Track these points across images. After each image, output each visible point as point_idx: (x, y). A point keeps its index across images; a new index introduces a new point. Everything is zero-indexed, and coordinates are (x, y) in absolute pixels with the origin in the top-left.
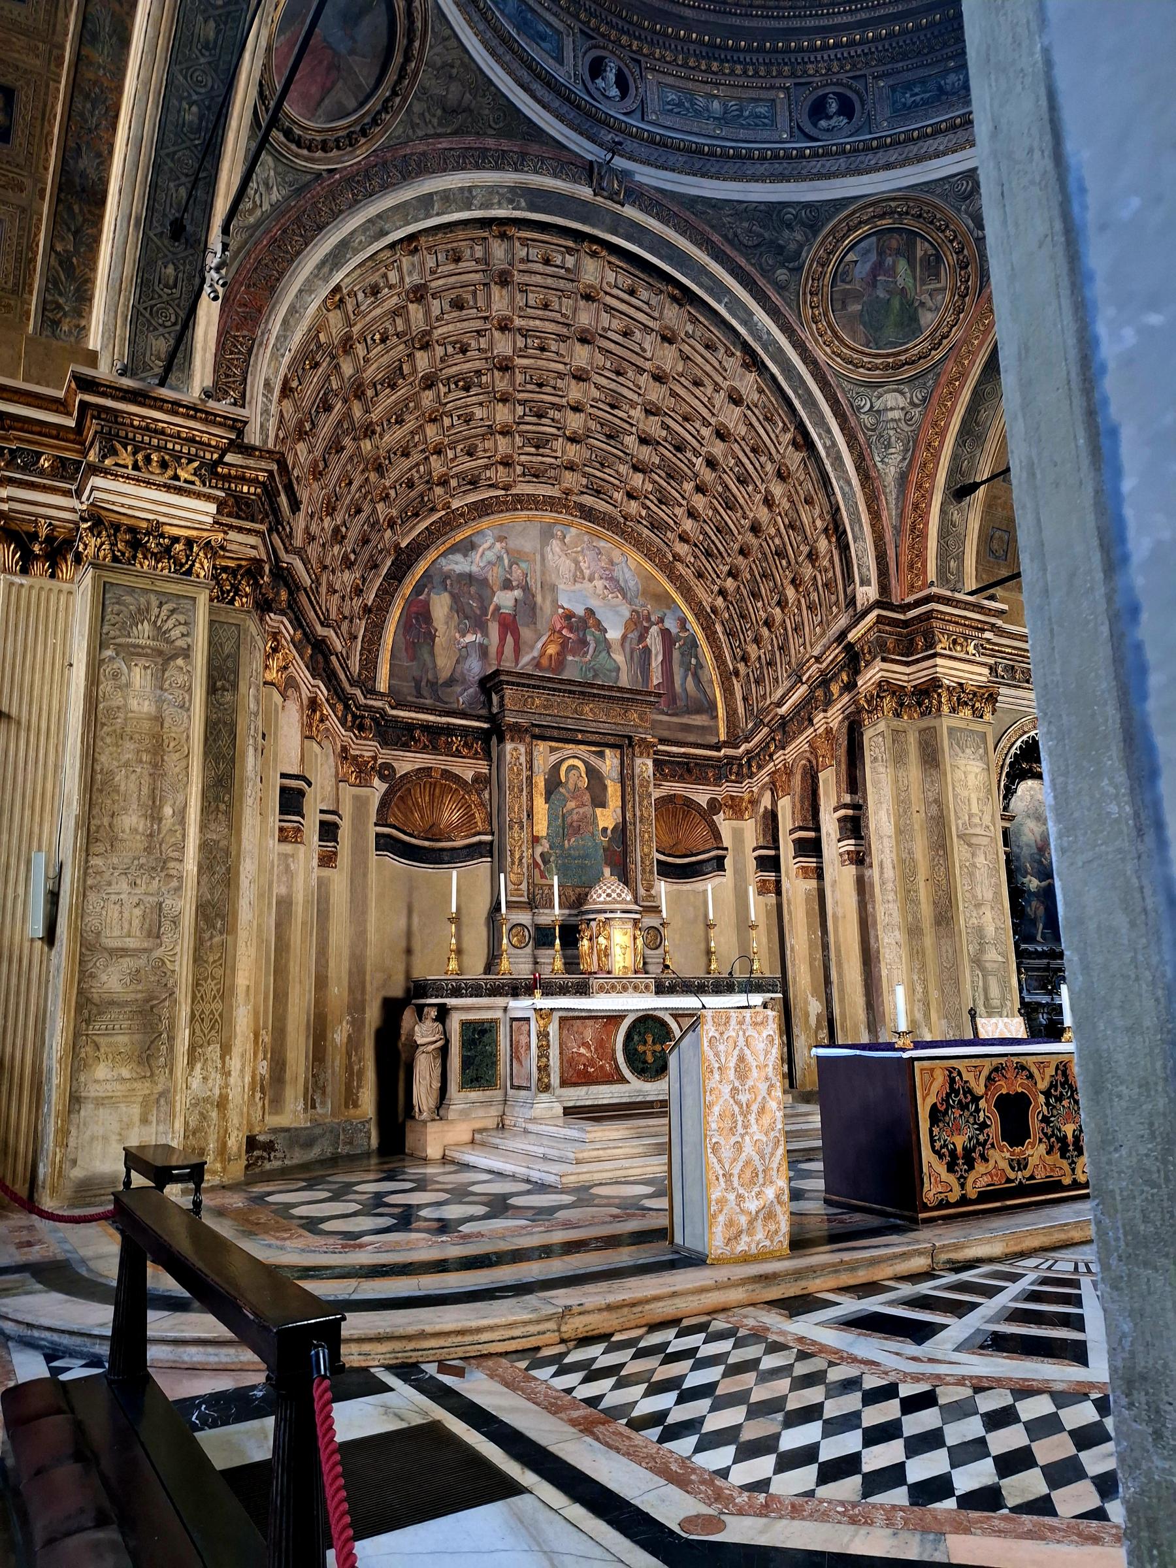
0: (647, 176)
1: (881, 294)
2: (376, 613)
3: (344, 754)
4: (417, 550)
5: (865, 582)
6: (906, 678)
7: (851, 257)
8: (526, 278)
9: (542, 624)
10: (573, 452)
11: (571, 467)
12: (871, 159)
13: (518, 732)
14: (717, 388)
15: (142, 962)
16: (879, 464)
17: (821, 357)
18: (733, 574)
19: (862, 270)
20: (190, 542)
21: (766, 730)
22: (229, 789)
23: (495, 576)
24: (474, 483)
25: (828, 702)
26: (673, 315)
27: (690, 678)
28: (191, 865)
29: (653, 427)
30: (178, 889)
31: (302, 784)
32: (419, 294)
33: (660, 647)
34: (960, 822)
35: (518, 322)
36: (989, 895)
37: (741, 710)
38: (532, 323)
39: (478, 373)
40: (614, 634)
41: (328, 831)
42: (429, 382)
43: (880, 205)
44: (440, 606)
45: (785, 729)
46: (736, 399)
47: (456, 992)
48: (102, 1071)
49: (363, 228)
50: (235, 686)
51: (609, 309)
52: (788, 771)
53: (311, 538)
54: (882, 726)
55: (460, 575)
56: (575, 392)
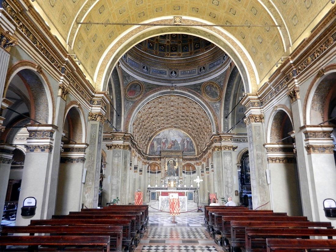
0: (178, 85)
1: (212, 91)
2: (147, 145)
3: (143, 162)
4: (152, 136)
5: (214, 131)
7: (206, 88)
8: (164, 102)
9: (169, 143)
10: (172, 120)
11: (172, 122)
12: (206, 76)
13: (163, 158)
14: (192, 108)
15: (116, 186)
16: (218, 113)
17: (207, 100)
18: (197, 131)
19: (209, 89)
20: (121, 145)
21: (202, 153)
22: (126, 168)
24: (159, 127)
25: (210, 149)
26: (184, 100)
27: (191, 147)
28: (121, 177)
29: (184, 114)
30: (119, 179)
32: (149, 108)
33: (186, 143)
34: (225, 166)
35: (163, 107)
36: (230, 176)
37: (199, 150)
38: (165, 107)
39: (159, 114)
40: (179, 142)
41: (141, 171)
42: (152, 117)
43: (207, 82)
44: (155, 143)
45: (205, 152)
46: (195, 109)
47: (151, 189)
48: (113, 195)
49: (141, 105)
50: (127, 158)
51: (175, 102)
52: (205, 159)
54: (215, 152)
55: (158, 138)
56: (172, 113)
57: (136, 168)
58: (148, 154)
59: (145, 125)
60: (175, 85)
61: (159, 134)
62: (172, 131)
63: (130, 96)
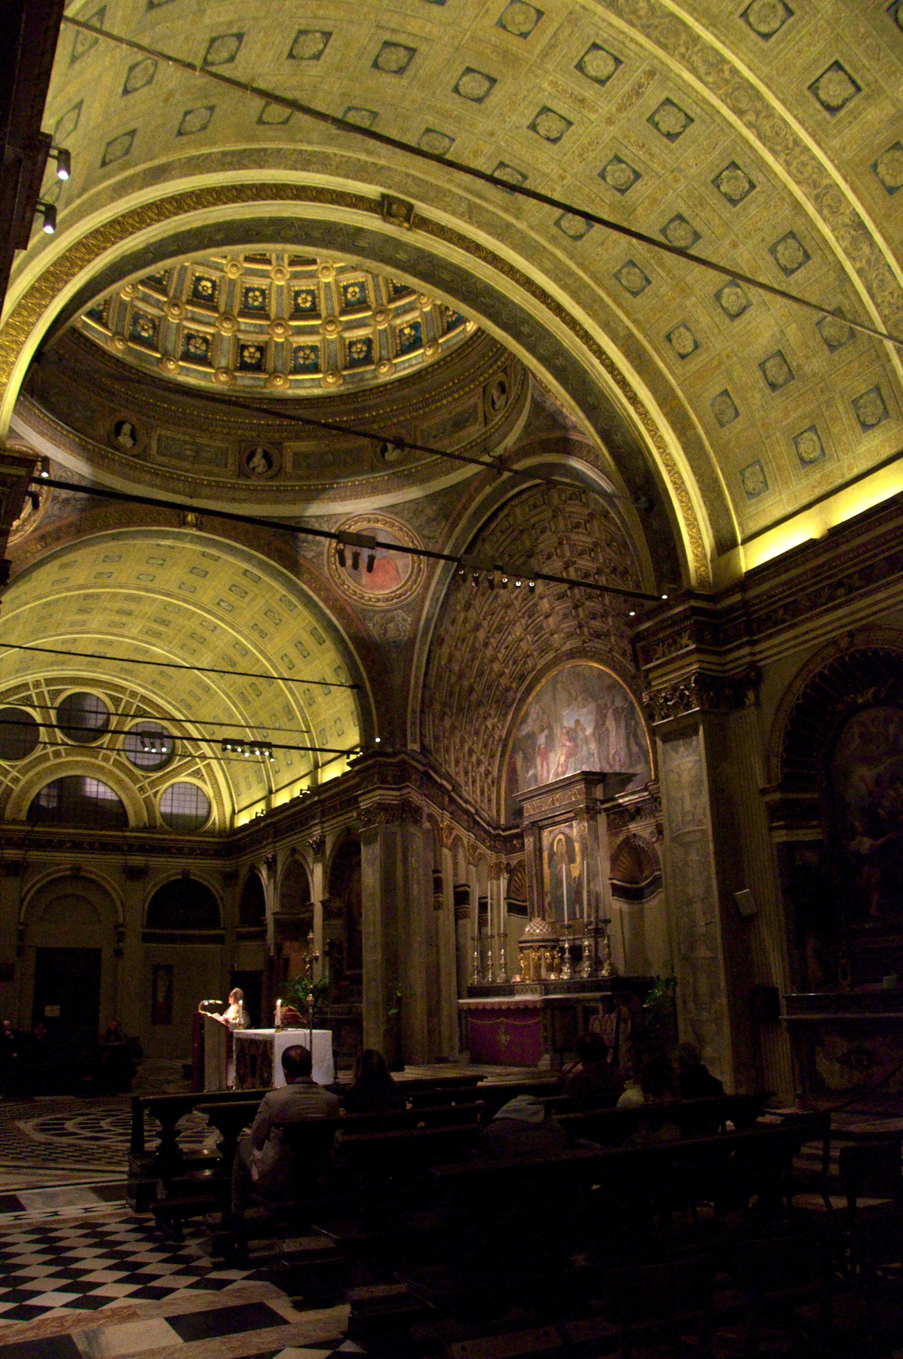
2: (497, 782)
6: (719, 668)
23: (536, 730)
39: (503, 618)
44: (519, 759)
53: (457, 762)
57: (462, 897)
58: (502, 821)
59: (471, 690)
60: (505, 450)
61: (527, 714)
63: (382, 587)
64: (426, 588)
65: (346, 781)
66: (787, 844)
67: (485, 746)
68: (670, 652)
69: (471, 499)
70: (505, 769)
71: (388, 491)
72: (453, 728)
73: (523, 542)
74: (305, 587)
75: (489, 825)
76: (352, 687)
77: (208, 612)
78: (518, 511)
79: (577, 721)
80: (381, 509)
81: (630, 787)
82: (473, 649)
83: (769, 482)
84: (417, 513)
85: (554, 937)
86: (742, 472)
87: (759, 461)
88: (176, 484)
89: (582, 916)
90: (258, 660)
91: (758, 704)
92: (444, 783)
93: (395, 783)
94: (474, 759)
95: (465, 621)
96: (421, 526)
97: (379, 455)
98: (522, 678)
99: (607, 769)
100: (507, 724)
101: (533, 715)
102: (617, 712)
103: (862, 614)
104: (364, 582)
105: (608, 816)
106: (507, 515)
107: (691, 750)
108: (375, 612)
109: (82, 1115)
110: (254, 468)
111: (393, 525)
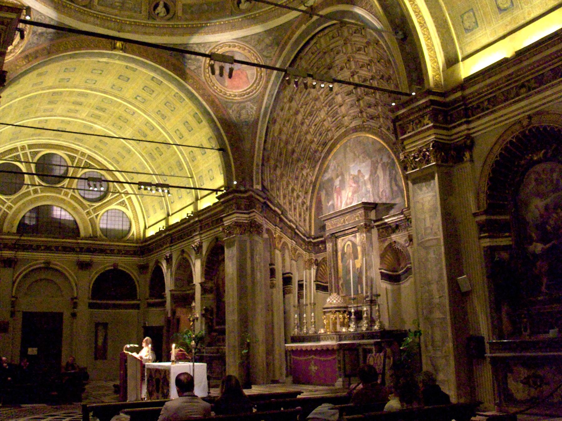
2: (309, 209)
6: (448, 138)
23: (334, 177)
31: (290, 275)
39: (313, 107)
53: (285, 196)
57: (287, 280)
58: (313, 233)
61: (328, 167)
62: (350, 146)
63: (238, 88)
64: (265, 88)
65: (215, 208)
66: (490, 247)
67: (302, 186)
68: (417, 128)
69: (293, 33)
70: (314, 200)
71: (241, 28)
72: (282, 175)
73: (325, 60)
74: (190, 88)
75: (305, 236)
76: (219, 150)
77: (130, 103)
78: (322, 40)
79: (359, 171)
80: (237, 39)
81: (392, 212)
82: (295, 126)
83: (479, 23)
84: (259, 41)
85: (345, 305)
86: (462, 16)
87: (472, 9)
88: (109, 23)
89: (362, 292)
90: (161, 133)
91: (472, 160)
92: (277, 209)
93: (246, 210)
94: (295, 194)
95: (290, 109)
96: (262, 49)
97: (236, 6)
98: (325, 144)
99: (378, 201)
100: (316, 173)
101: (332, 167)
102: (384, 165)
103: (535, 105)
104: (226, 84)
105: (378, 230)
106: (316, 43)
107: (430, 189)
108: (234, 103)
109: (51, 416)
110: (158, 14)
111: (245, 49)
